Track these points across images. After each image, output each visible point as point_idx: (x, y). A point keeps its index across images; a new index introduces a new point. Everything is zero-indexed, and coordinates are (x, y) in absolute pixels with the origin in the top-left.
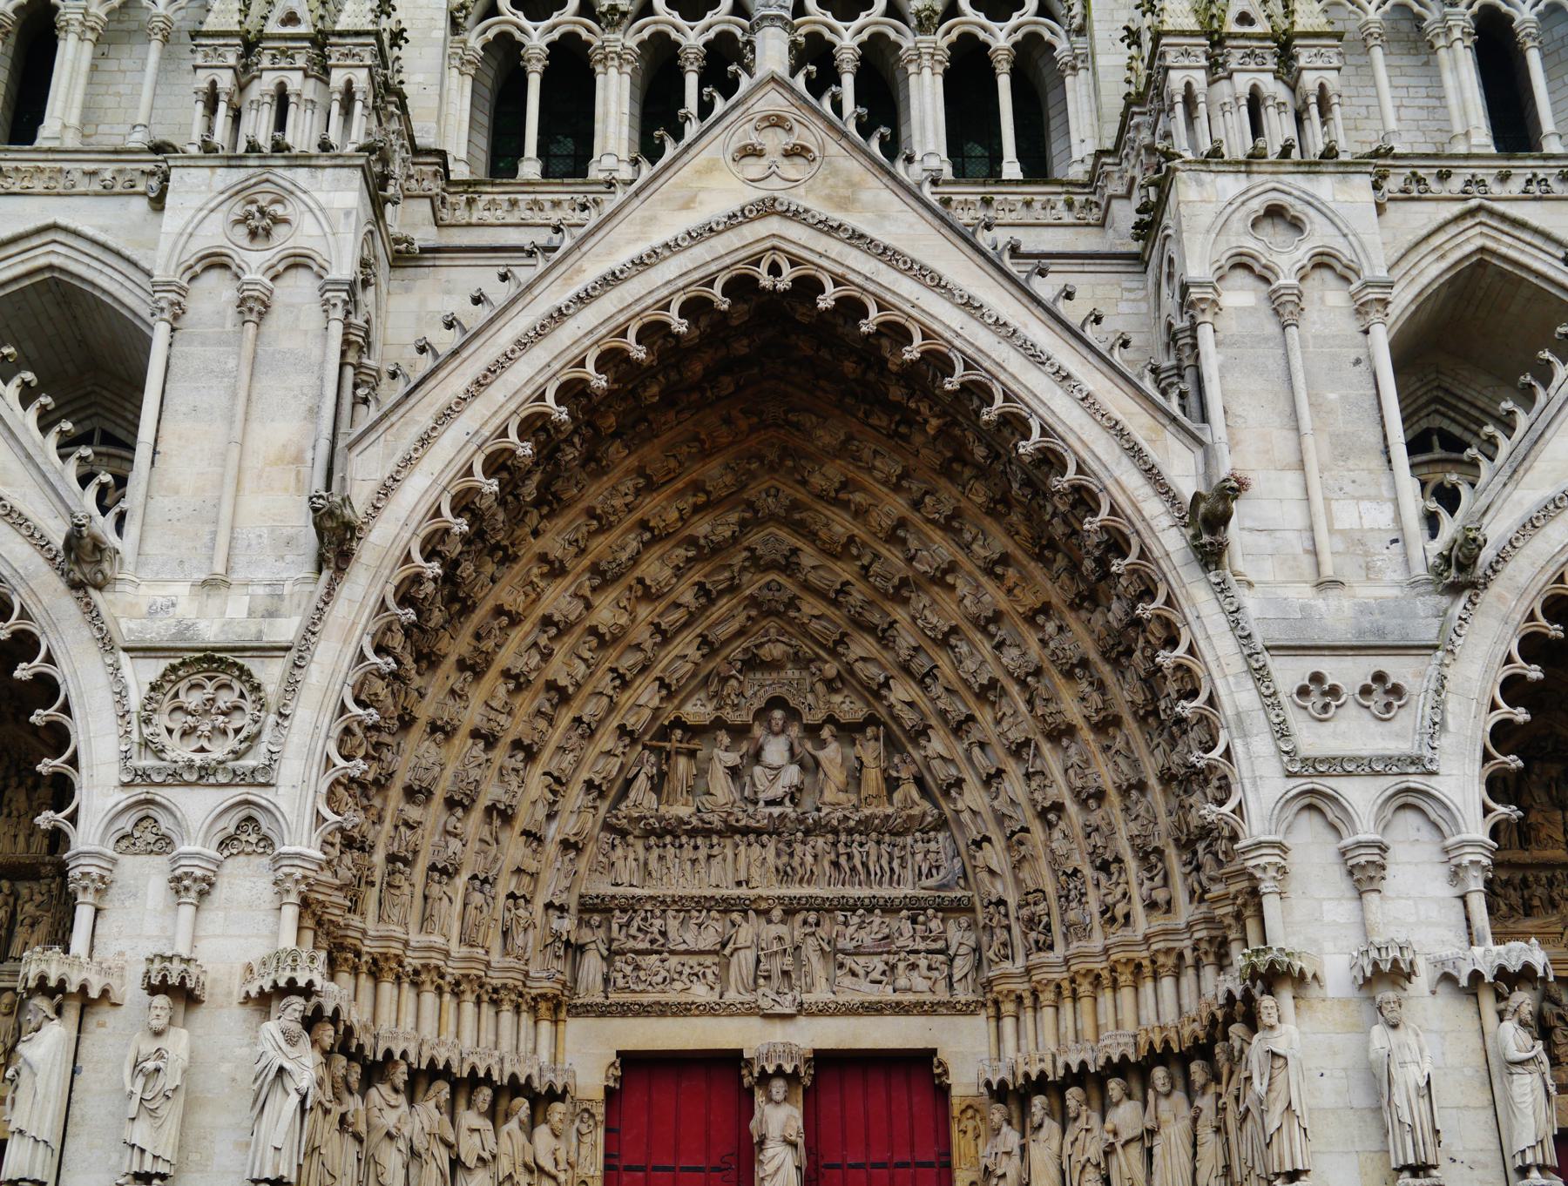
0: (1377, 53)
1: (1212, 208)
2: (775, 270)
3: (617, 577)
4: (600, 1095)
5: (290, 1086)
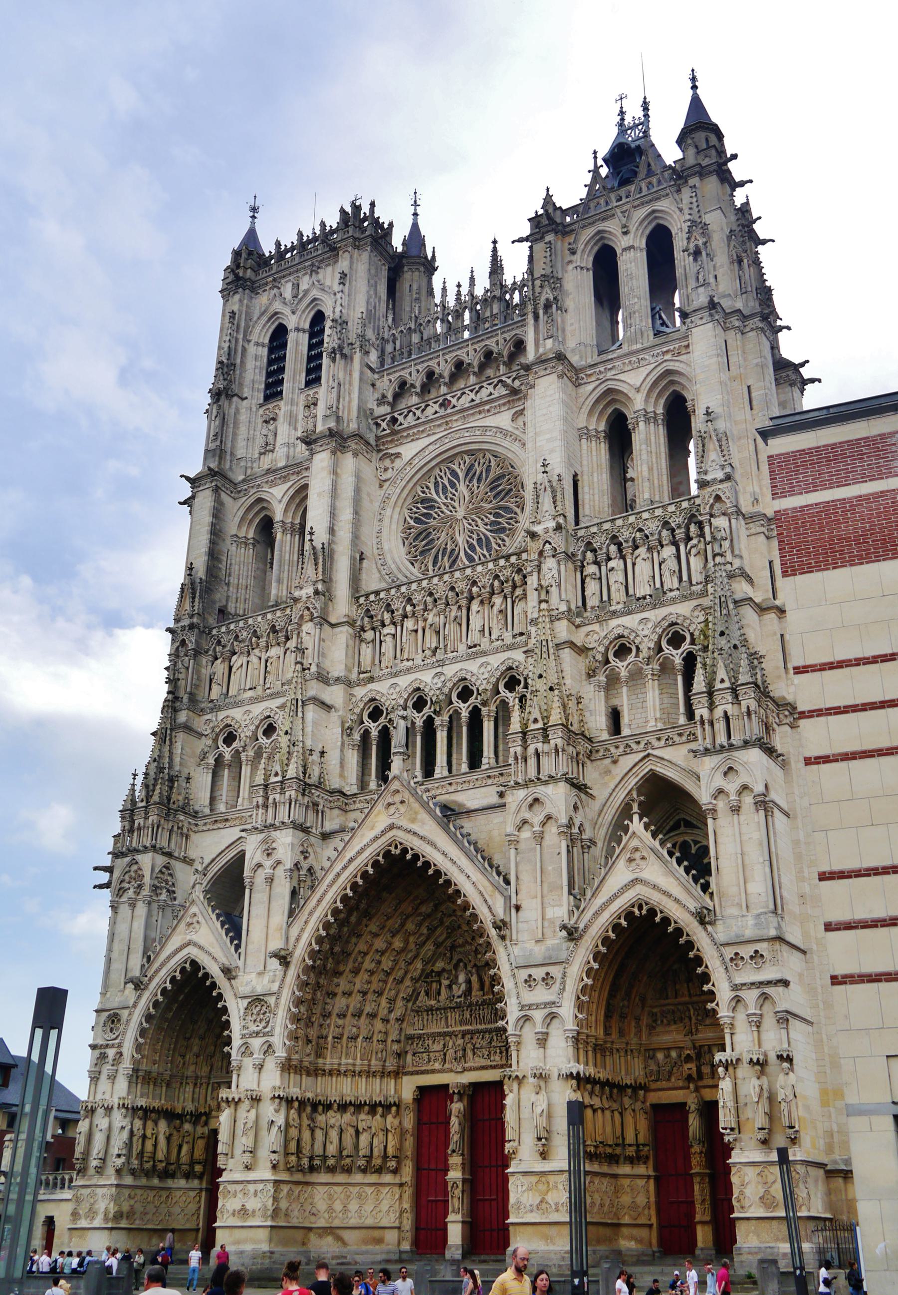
0: (625, 689)
1: (516, 804)
2: (396, 847)
3: (398, 932)
4: (411, 1101)
5: (276, 1124)
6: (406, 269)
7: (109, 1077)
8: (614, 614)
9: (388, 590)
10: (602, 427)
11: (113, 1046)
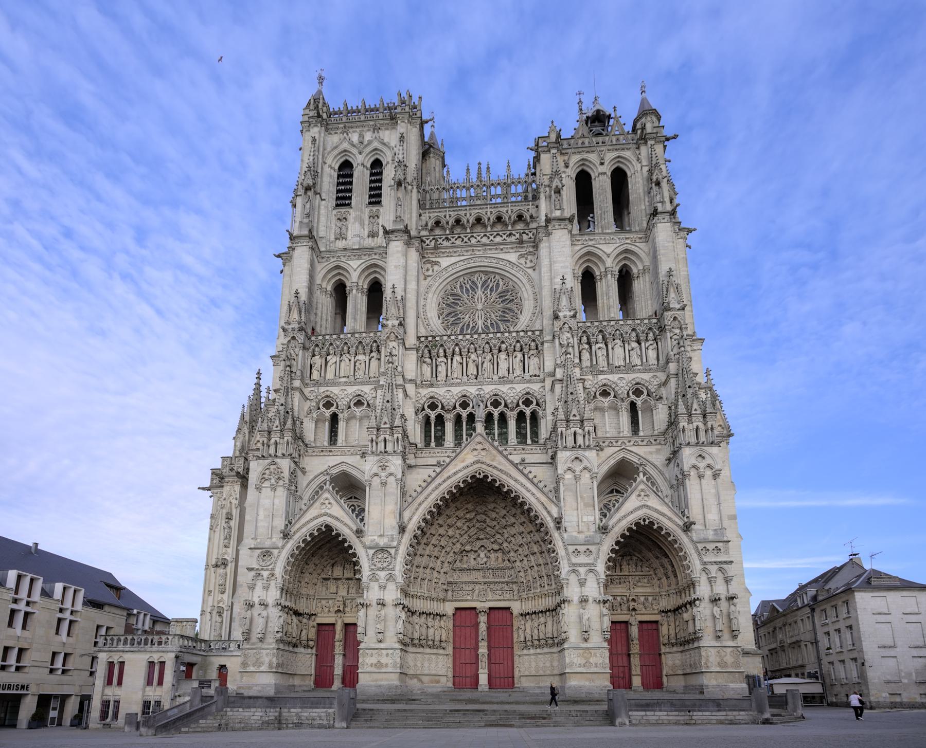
0: (606, 413)
2: (480, 474)
6: (431, 155)
7: (264, 587)
8: (603, 372)
9: (441, 336)
10: (580, 274)
11: (267, 570)
